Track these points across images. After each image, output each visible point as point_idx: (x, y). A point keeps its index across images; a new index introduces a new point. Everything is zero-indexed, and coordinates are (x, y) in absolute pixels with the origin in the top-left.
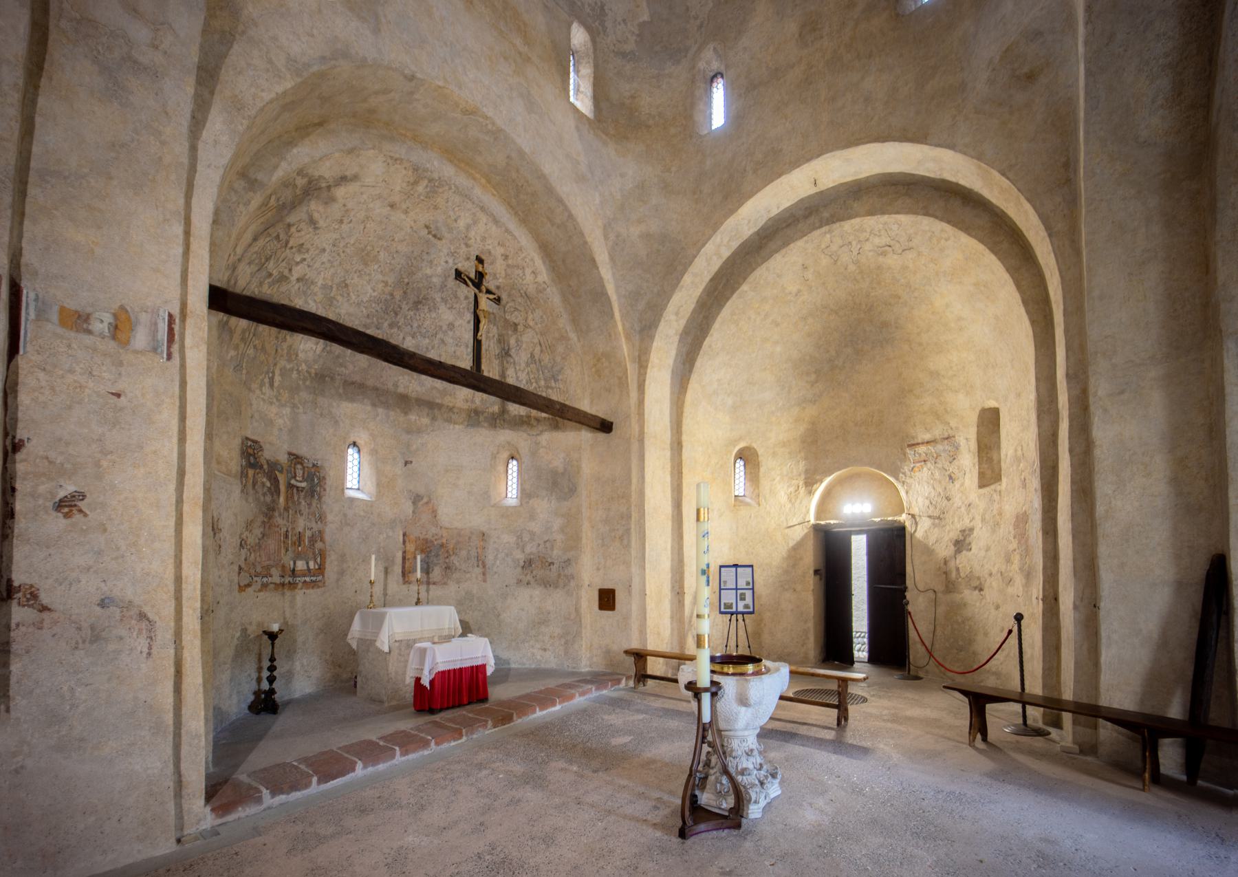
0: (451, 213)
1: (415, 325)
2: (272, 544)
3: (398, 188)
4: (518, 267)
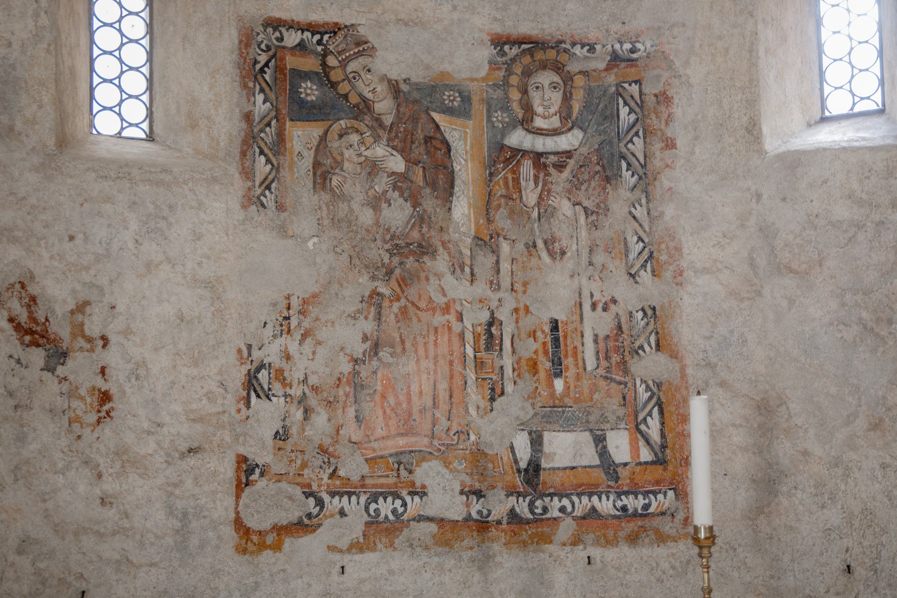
2: (418, 375)
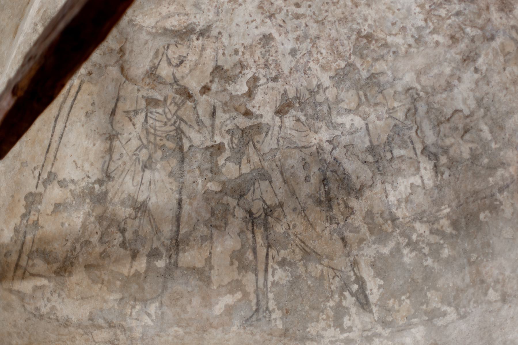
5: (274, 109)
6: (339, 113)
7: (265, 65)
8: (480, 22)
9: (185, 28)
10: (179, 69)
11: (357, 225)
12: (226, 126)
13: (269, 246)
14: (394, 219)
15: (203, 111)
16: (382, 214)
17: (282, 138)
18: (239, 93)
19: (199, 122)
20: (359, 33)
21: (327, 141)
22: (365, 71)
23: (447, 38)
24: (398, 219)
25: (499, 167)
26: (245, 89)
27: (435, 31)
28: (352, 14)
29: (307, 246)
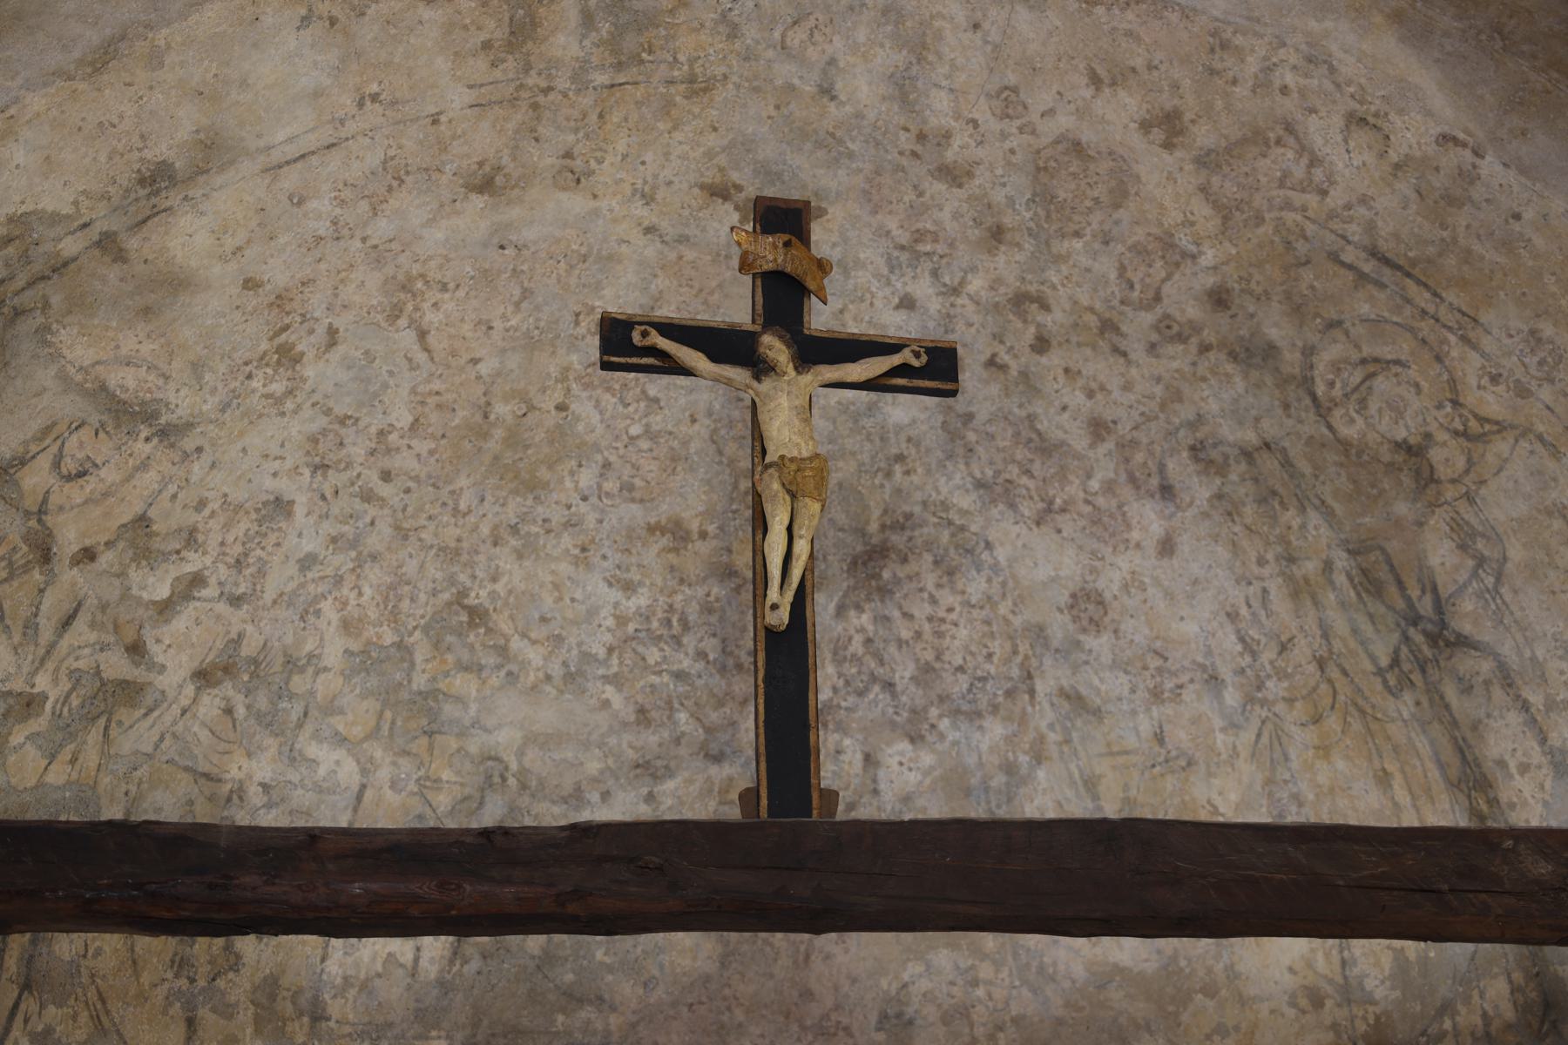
0: (785, 71)
1: (904, 672)
3: (457, 98)
4: (1257, 139)
5: (196, 664)
6: (316, 736)
7: (238, 561)
8: (714, 717)
9: (143, 403)
10: (68, 486)
11: (233, 999)
12: (77, 659)
13: (26, 986)
14: (317, 1015)
15: (52, 604)
16: (297, 994)
17: (174, 735)
18: (145, 595)
19: (31, 627)
20: (463, 593)
21: (260, 784)
22: (426, 676)
23: (631, 708)
24: (328, 1019)
25: (590, 1002)
26: (163, 592)
27: (615, 680)
28: (477, 552)
29: (108, 1012)
